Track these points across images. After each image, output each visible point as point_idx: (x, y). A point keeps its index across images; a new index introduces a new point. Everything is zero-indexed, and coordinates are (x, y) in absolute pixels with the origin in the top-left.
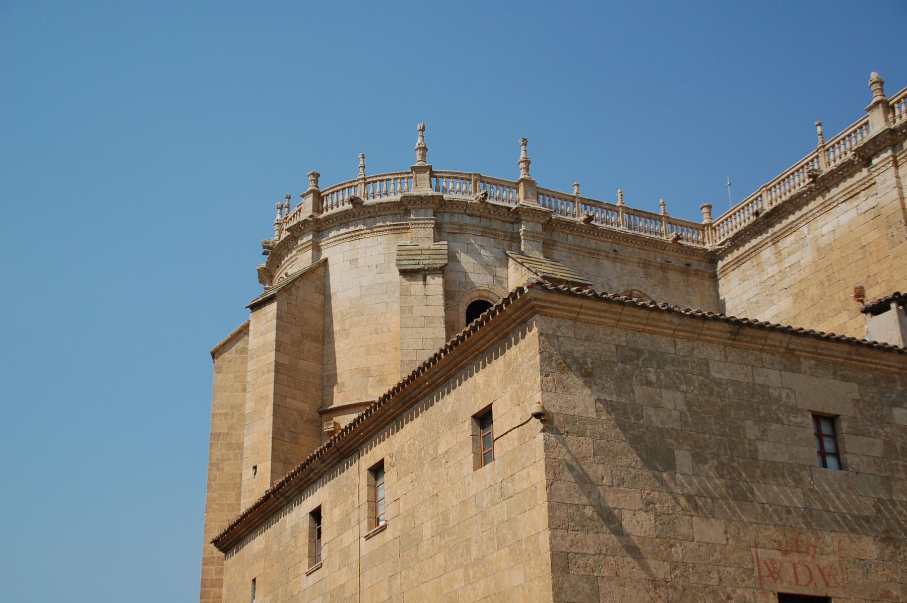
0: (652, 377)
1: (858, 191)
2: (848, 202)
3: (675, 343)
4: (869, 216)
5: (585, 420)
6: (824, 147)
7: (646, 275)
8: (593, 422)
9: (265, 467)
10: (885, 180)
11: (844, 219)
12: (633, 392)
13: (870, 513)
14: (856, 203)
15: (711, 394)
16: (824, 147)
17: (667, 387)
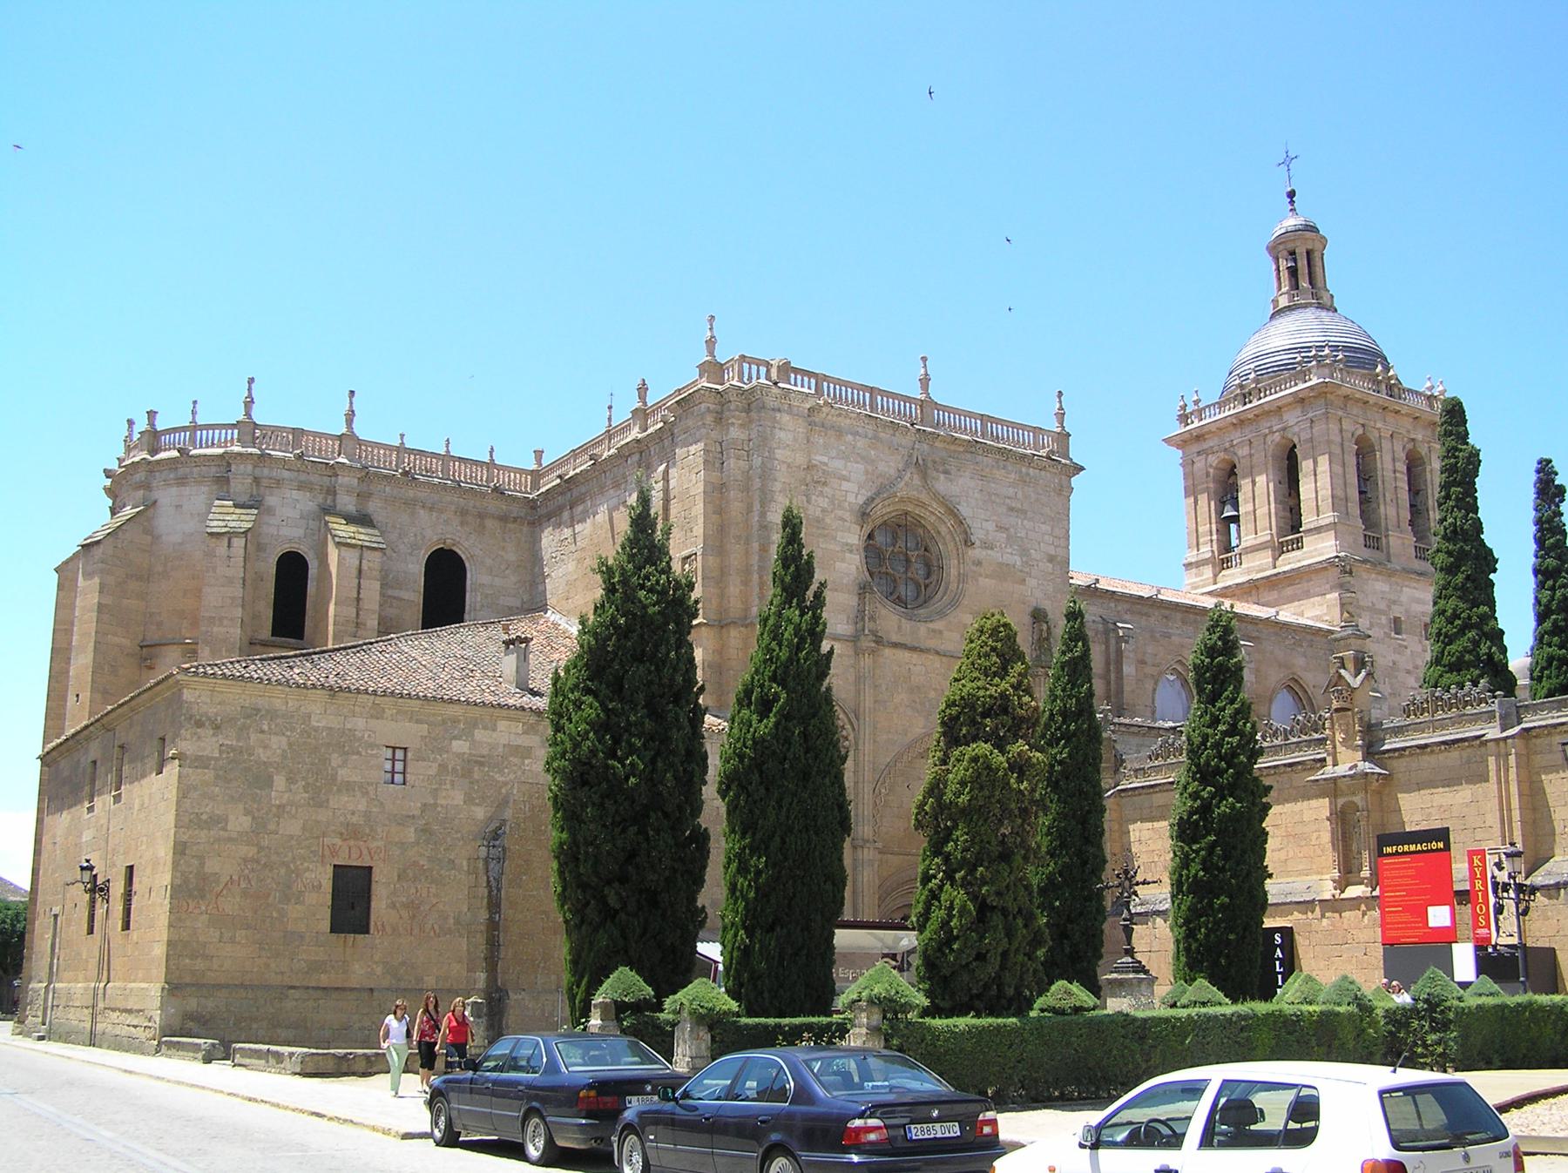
0: (265, 727)
3: (287, 703)
5: (210, 759)
7: (462, 524)
8: (216, 759)
9: (86, 696)
12: (249, 738)
13: (417, 813)
15: (309, 737)
17: (275, 734)
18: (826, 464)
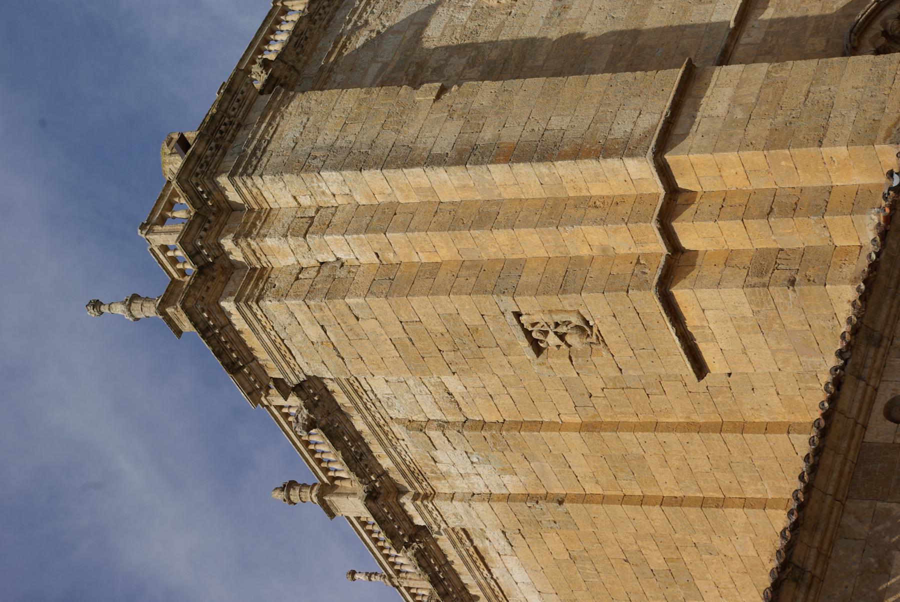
1: (472, 549)
2: (490, 565)
4: (518, 540)
6: (390, 577)
10: (456, 515)
11: (520, 575)
14: (494, 555)
16: (390, 577)
18: (382, 69)
